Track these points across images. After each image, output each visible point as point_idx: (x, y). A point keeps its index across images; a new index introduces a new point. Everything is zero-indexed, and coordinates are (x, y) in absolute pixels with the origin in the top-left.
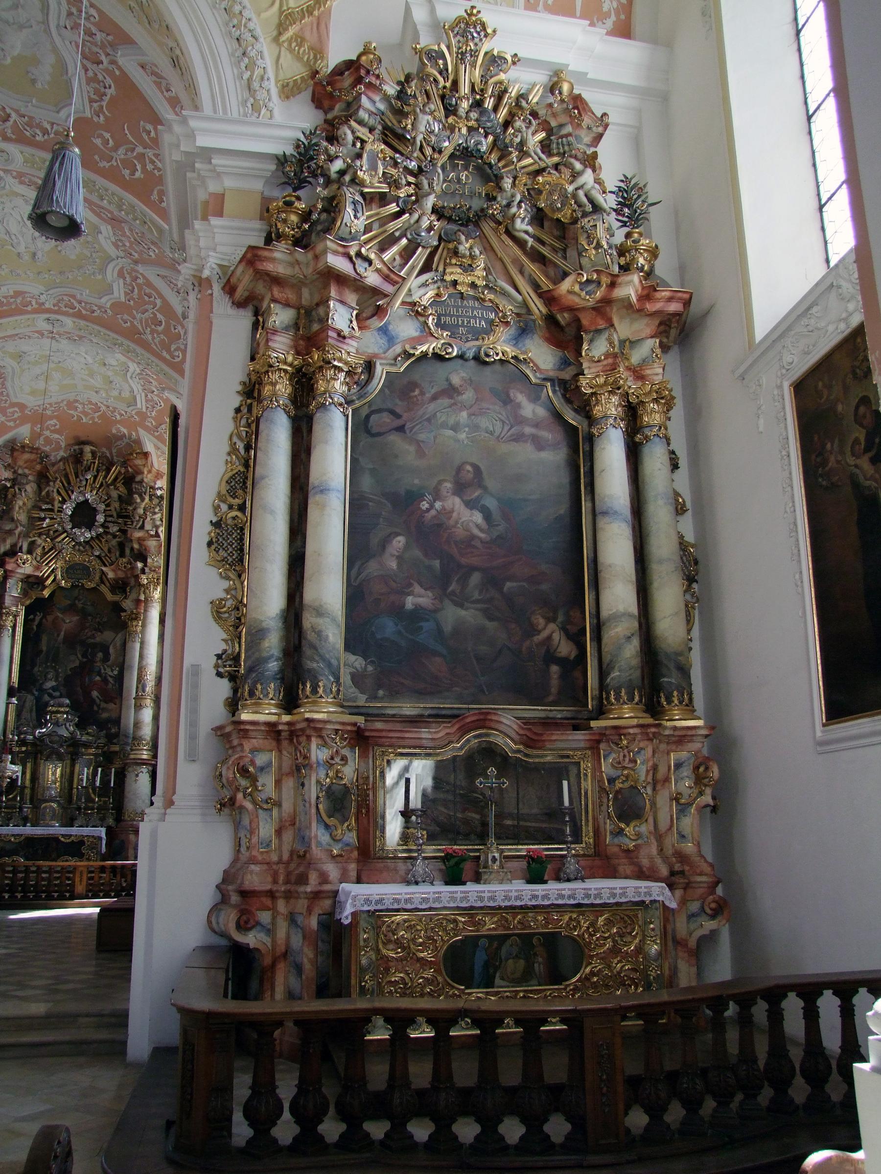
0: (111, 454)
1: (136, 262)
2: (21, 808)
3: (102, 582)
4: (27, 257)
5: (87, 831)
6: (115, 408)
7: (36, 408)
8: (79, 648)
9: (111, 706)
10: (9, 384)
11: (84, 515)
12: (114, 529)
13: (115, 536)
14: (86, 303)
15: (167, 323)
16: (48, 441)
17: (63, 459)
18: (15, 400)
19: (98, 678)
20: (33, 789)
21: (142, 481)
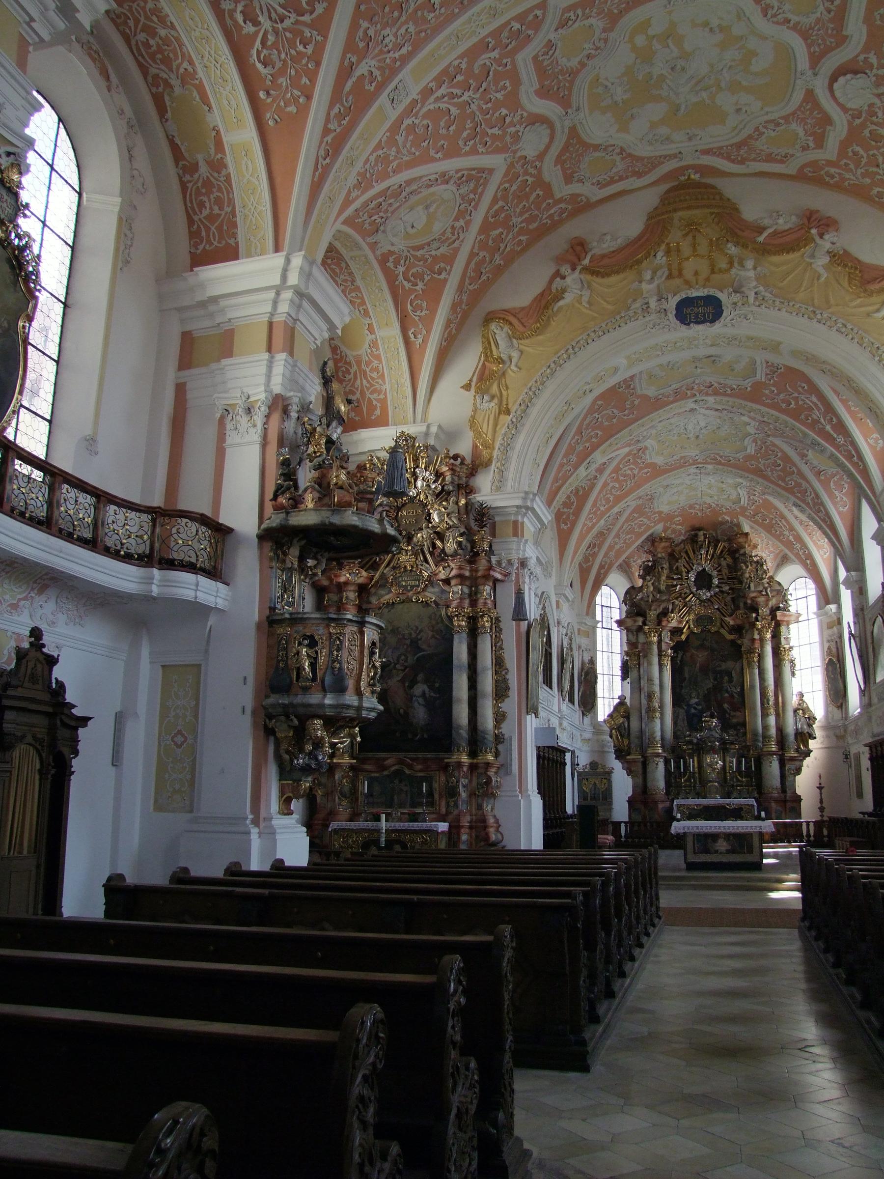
0: (716, 533)
2: (694, 787)
3: (723, 627)
5: (742, 801)
8: (711, 674)
9: (738, 714)
10: (655, 501)
11: (703, 580)
12: (726, 588)
13: (728, 594)
16: (674, 531)
17: (683, 541)
19: (727, 695)
20: (699, 773)
21: (744, 554)
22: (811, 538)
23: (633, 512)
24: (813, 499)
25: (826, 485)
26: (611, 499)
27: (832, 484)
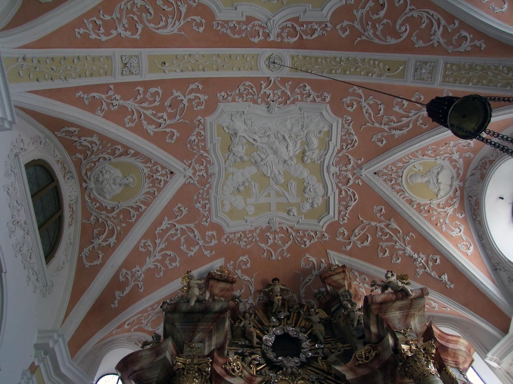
0: (299, 297)
6: (304, 231)
7: (232, 236)
10: (213, 193)
18: (215, 220)
22: (440, 230)
23: (179, 197)
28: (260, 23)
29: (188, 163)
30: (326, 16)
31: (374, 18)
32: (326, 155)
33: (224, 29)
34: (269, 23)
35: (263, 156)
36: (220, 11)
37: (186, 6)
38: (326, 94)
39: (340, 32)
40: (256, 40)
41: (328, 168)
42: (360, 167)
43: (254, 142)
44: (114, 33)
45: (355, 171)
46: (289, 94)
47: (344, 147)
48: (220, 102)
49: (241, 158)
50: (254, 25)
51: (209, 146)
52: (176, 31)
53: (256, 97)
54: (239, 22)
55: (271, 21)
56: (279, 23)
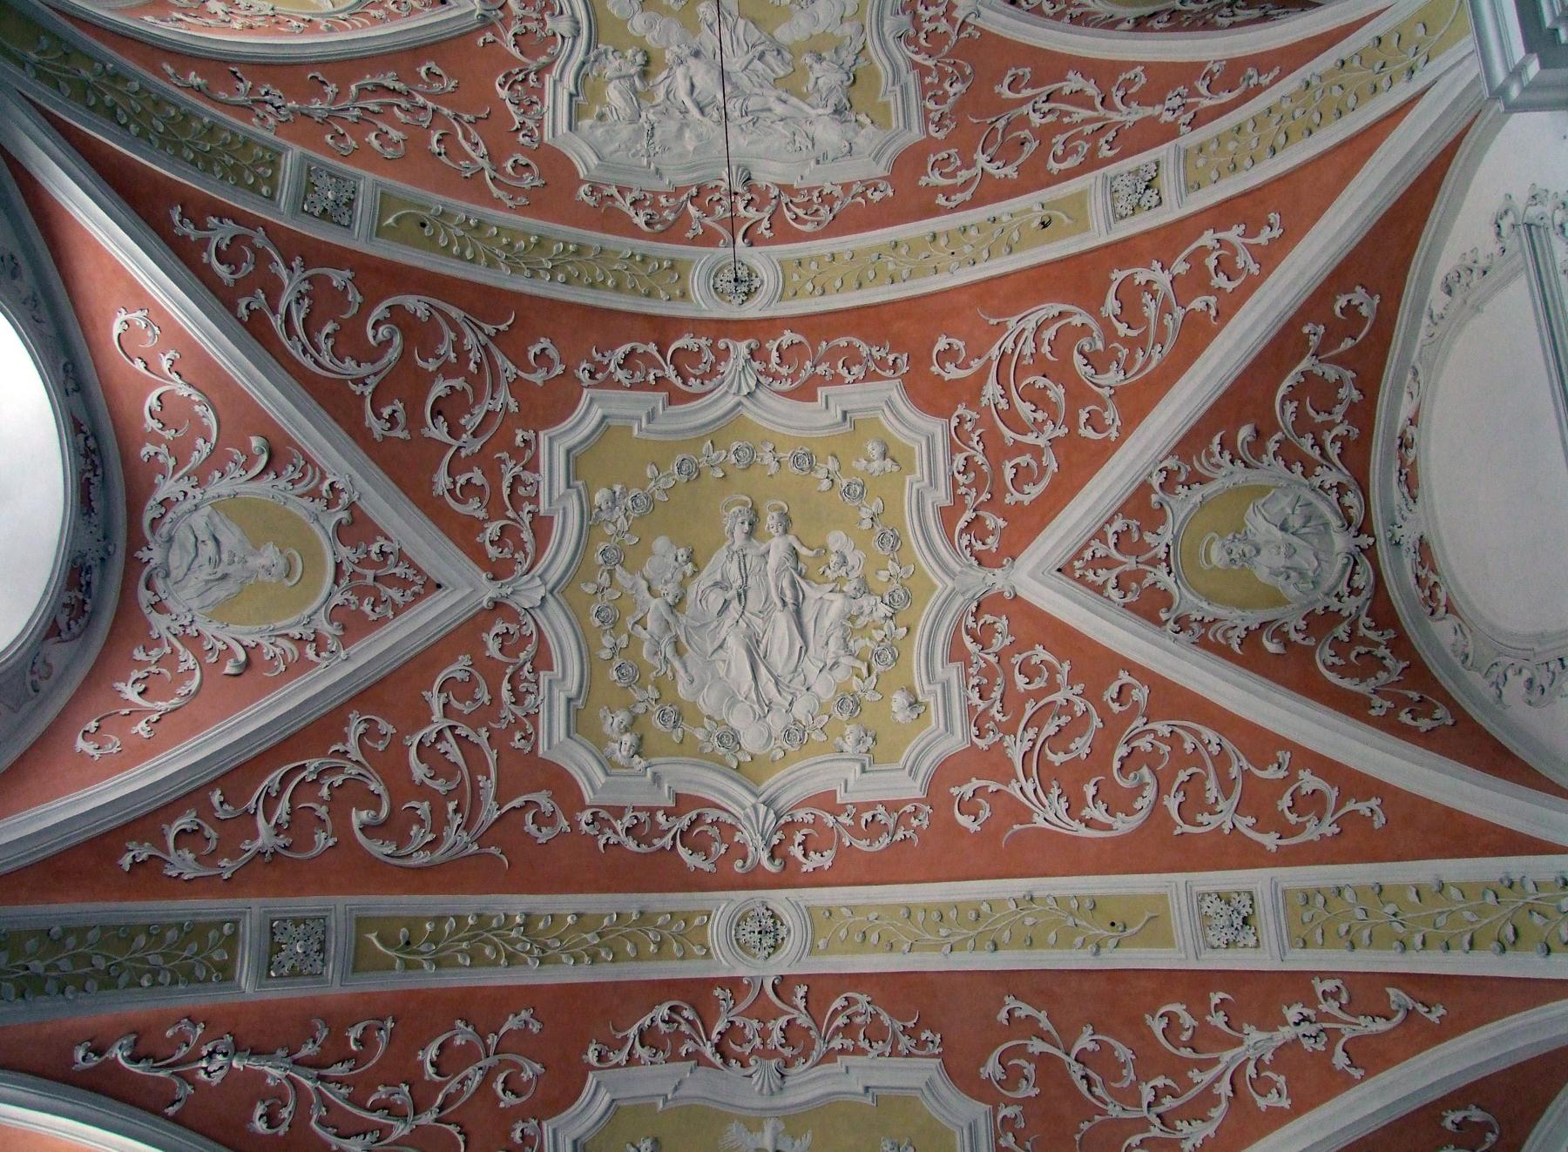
1: (497, 605)
4: (771, 520)
14: (643, 386)
15: (415, 421)
24: (273, 291)
25: (241, 416)
26: (1111, 305)
27: (211, 420)
28: (776, 385)
29: (970, 30)
30: (592, 401)
31: (461, 379)
32: (583, 63)
33: (877, 355)
34: (753, 383)
35: (758, 65)
36: (889, 403)
37: (984, 402)
38: (591, 201)
39: (553, 353)
40: (788, 337)
41: (578, 31)
42: (486, 23)
43: (784, 96)
44: (1180, 267)
45: (501, 14)
46: (692, 210)
47: (532, 76)
48: (884, 178)
49: (820, 59)
50: (793, 377)
51: (911, 78)
52: (1012, 322)
53: (785, 199)
54: (837, 380)
55: (745, 391)
56: (723, 388)
